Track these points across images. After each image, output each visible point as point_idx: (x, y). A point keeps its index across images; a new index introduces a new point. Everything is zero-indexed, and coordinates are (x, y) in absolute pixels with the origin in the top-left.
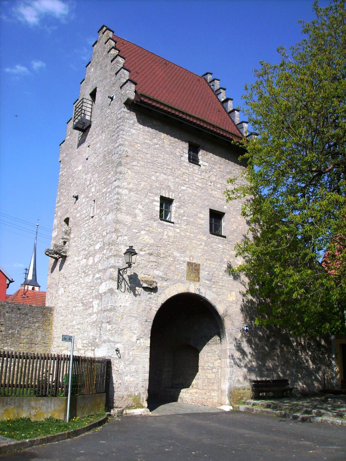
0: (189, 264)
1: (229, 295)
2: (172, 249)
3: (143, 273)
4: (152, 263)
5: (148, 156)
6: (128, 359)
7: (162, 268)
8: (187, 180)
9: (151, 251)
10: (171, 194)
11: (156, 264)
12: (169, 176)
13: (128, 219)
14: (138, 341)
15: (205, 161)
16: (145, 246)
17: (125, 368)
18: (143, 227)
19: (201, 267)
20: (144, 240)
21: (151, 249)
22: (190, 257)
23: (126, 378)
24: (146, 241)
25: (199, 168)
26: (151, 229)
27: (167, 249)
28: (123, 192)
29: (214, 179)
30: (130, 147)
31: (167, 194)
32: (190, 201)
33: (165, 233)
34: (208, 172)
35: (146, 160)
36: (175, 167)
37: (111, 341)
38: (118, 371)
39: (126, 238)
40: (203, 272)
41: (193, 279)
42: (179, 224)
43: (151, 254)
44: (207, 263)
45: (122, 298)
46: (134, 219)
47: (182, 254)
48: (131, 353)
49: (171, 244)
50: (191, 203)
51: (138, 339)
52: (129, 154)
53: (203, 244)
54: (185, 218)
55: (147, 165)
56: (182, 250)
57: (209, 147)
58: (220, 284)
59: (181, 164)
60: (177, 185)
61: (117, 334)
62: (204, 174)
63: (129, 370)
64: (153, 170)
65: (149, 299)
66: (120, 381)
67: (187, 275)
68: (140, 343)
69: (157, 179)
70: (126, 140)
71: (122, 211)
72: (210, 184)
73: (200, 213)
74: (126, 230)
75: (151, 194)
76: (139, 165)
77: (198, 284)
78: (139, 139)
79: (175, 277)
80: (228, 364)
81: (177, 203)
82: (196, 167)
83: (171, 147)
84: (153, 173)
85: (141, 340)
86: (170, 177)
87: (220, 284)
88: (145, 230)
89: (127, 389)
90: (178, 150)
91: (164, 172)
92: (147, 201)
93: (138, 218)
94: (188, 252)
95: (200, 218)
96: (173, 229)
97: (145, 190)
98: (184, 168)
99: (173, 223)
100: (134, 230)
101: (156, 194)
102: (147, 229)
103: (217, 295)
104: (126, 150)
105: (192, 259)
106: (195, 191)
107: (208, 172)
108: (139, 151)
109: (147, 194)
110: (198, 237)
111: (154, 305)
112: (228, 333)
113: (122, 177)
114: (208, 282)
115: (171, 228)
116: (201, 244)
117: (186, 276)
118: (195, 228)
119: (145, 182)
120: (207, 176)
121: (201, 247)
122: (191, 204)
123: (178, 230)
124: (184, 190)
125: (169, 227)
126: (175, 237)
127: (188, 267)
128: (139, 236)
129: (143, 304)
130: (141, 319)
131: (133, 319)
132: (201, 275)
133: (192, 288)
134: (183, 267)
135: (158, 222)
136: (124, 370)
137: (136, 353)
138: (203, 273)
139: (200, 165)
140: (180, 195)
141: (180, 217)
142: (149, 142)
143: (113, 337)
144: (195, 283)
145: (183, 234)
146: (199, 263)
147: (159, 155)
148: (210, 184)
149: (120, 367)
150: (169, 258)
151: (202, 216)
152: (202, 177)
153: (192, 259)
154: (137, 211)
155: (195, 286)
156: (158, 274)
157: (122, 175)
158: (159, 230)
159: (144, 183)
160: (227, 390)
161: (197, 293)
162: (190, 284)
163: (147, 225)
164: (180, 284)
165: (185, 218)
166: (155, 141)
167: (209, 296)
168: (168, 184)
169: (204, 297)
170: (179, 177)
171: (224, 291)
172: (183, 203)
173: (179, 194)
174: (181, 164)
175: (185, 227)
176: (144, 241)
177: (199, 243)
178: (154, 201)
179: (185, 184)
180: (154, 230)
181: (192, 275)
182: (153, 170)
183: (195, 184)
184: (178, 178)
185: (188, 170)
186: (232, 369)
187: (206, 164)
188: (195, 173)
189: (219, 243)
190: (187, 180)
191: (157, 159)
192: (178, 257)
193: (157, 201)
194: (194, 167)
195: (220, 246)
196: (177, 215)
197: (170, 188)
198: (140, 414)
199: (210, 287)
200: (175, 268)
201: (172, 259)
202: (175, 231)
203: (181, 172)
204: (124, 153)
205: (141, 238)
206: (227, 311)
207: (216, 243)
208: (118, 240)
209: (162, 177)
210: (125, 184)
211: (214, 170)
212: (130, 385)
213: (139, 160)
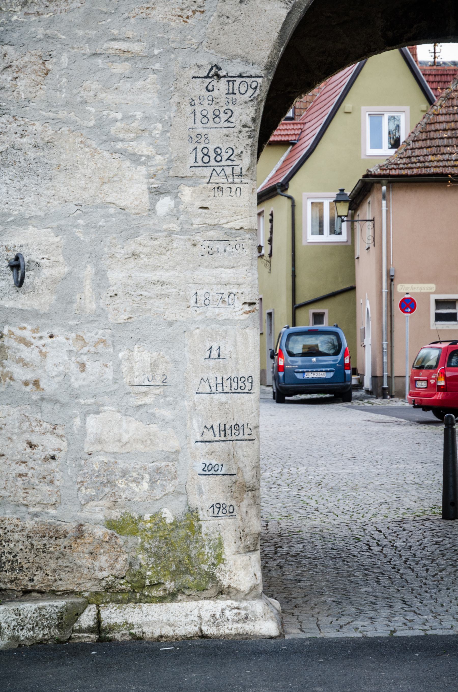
6: (100, 314)
14: (165, 204)
17: (83, 367)
23: (92, 422)
38: (36, 383)
48: (116, 276)
51: (157, 192)
63: (109, 374)
66: (51, 443)
68: (174, 214)
85: (187, 193)
89: (106, 481)
136: (78, 381)
149: (49, 362)
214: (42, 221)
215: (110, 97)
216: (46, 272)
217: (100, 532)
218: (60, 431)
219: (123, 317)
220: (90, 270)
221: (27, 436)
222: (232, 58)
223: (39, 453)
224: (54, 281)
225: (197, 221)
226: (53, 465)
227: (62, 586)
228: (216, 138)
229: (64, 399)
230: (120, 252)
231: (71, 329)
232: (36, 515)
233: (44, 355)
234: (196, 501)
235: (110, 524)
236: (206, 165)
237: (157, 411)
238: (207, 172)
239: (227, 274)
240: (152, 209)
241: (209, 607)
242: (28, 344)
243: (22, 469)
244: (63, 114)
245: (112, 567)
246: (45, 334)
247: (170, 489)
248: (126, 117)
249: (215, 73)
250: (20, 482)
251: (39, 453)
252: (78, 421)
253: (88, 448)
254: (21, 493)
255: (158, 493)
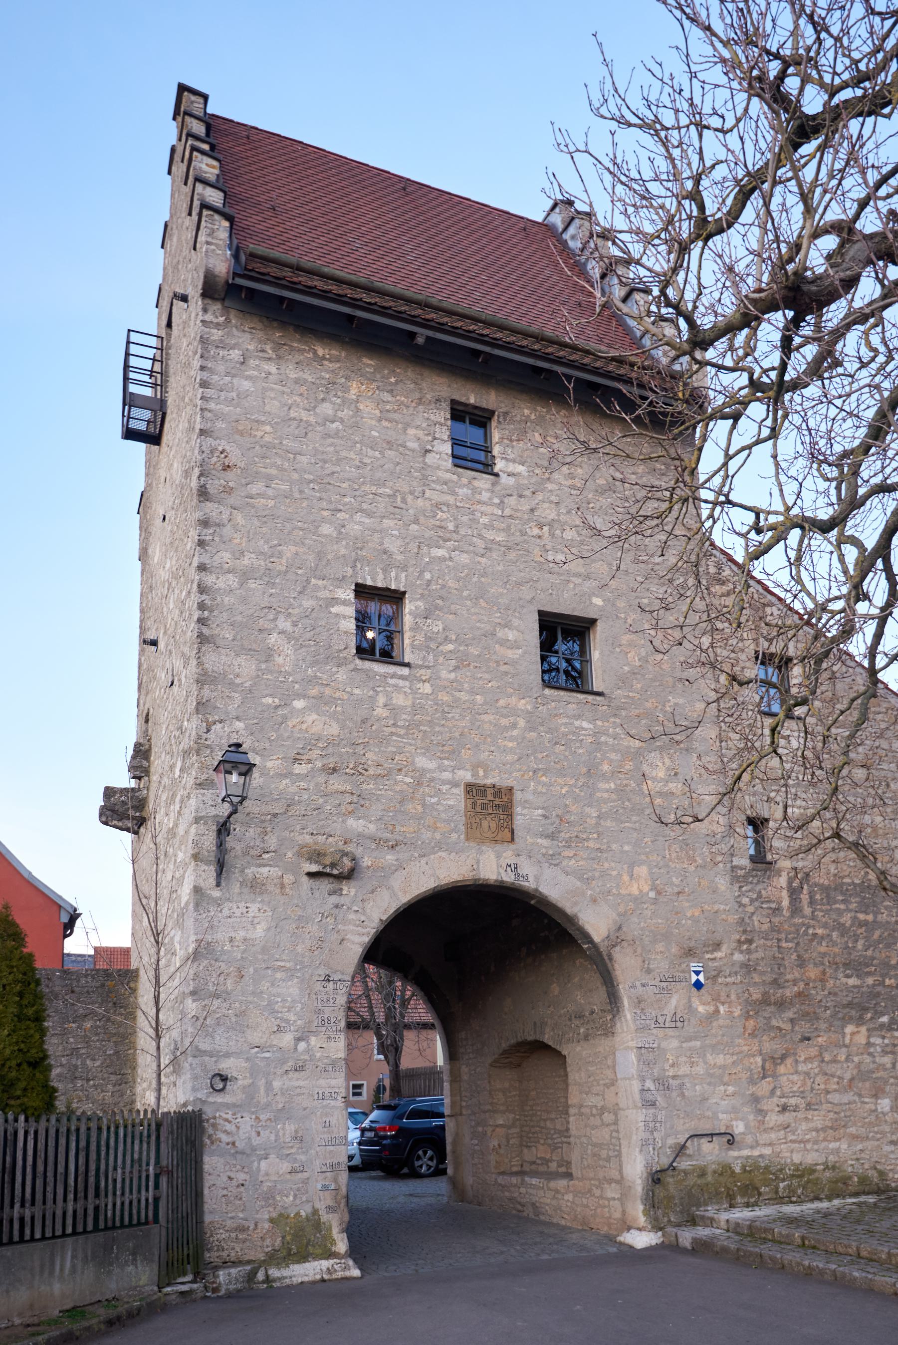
0: (472, 789)
1: (626, 878)
2: (408, 748)
3: (309, 830)
4: (340, 796)
5: (304, 459)
6: (268, 1105)
7: (376, 810)
8: (451, 526)
9: (331, 762)
10: (393, 574)
11: (355, 799)
12: (383, 517)
13: (245, 668)
14: (302, 1046)
15: (514, 461)
16: (310, 745)
17: (258, 1134)
18: (297, 686)
19: (518, 796)
20: (304, 726)
21: (332, 754)
22: (475, 768)
23: (264, 1164)
24: (314, 730)
25: (493, 485)
26: (328, 691)
27: (390, 749)
28: (221, 584)
29: (548, 513)
30: (237, 437)
31: (381, 576)
32: (465, 594)
33: (381, 700)
34: (527, 493)
35: (295, 476)
36: (406, 489)
37: (204, 1053)
38: (233, 1144)
39: (239, 725)
40: (525, 812)
41: (489, 835)
42: (428, 667)
43: (334, 770)
44: (539, 782)
45: (238, 913)
46: (263, 666)
47: (446, 762)
48: (277, 1084)
49: (402, 732)
50: (468, 597)
51: (298, 1040)
52: (232, 459)
53: (522, 723)
54: (451, 647)
55: (301, 492)
56: (446, 749)
57: (526, 412)
58: (591, 844)
59: (425, 477)
60: (413, 547)
61: (222, 1028)
62: (512, 501)
63: (273, 1138)
64: (324, 504)
65: (336, 911)
66: (241, 1177)
67: (469, 826)
68: (308, 1051)
69: (340, 533)
70: (218, 416)
71: (220, 642)
72: (536, 531)
73: (507, 625)
74: (237, 702)
75: (320, 583)
76: (270, 492)
77: (508, 855)
78: (267, 408)
79: (426, 835)
80: (637, 1096)
81: (420, 603)
82: (483, 481)
83: (385, 423)
84: (325, 513)
85: (313, 1040)
86: (387, 522)
87: (591, 844)
88: (304, 697)
89: (269, 1197)
90: (411, 431)
91: (365, 506)
92: (308, 603)
93: (280, 660)
94: (465, 754)
95: (504, 642)
96: (407, 683)
97: (300, 572)
98: (438, 487)
99: (407, 665)
100: (269, 700)
101: (341, 581)
102: (314, 692)
103: (580, 879)
104: (220, 449)
105: (481, 773)
106: (483, 560)
107: (527, 493)
108: (268, 446)
109: (308, 582)
110: (502, 703)
111: (351, 927)
112: (630, 997)
113: (212, 534)
114: (544, 842)
115: (401, 683)
116: (514, 726)
117: (463, 828)
118: (487, 676)
119: (295, 544)
120: (526, 507)
121: (515, 733)
122: (468, 603)
123: (427, 688)
124: (442, 559)
125: (392, 681)
126: (416, 709)
127: (470, 802)
128: (285, 718)
129: (313, 928)
130: (307, 976)
131: (279, 975)
132: (519, 821)
133: (490, 866)
134: (451, 802)
135: (352, 666)
136: (256, 1141)
137: (297, 1084)
138: (522, 817)
139: (497, 475)
140: (428, 576)
141: (433, 645)
142: (304, 415)
143: (208, 1040)
144: (499, 847)
145: (444, 697)
146: (510, 783)
147: (344, 454)
148: (536, 531)
149: (241, 1132)
150: (399, 778)
151: (511, 635)
152: (507, 512)
153: (481, 773)
154: (273, 639)
155: (498, 857)
156: (360, 830)
157: (211, 531)
158: (357, 691)
159: (293, 549)
160: (639, 1181)
161: (508, 878)
162: (481, 852)
163: (312, 681)
164: (443, 854)
165: (451, 647)
166: (326, 409)
167: (552, 884)
168: (381, 544)
169: (536, 890)
170: (422, 519)
171: (606, 865)
172: (440, 602)
173: (422, 572)
174: (425, 477)
175: (452, 676)
176: (306, 731)
177: (504, 722)
178: (335, 601)
179: (445, 541)
180: (338, 695)
181: (485, 824)
182: (324, 504)
183: (480, 536)
184: (416, 521)
185: (454, 493)
186: (652, 1111)
187: (520, 469)
188: (479, 502)
189: (579, 717)
190: (451, 526)
191: (338, 469)
192: (430, 771)
193: (345, 603)
194: (476, 483)
195: (585, 724)
196: (420, 638)
197: (390, 556)
198: (318, 1277)
199: (553, 859)
200: (424, 806)
201: (408, 780)
202: (414, 692)
203: (428, 504)
204: (214, 459)
205: (295, 721)
206: (620, 928)
207: (568, 717)
208: (212, 735)
209: (357, 525)
210: (226, 556)
211: (550, 486)
212: (279, 1187)
213: (270, 478)
214: (237, 1054)
215: (274, 990)
216: (240, 1082)
217: (267, 1225)
218: (246, 1170)
219: (280, 1106)
220: (263, 1080)
221: (229, 1173)
222: (335, 972)
223: (234, 1183)
224: (244, 1087)
225: (318, 1055)
226: (242, 1189)
227: (246, 1258)
228: (328, 1012)
229: (248, 1151)
230: (279, 1072)
231: (253, 1113)
232: (232, 1218)
233: (238, 1128)
234: (318, 1205)
235: (271, 1220)
236: (323, 1025)
237: (298, 1157)
238: (324, 1029)
239: (333, 1082)
240: (296, 1049)
241: (325, 1264)
242: (230, 1122)
243: (225, 1192)
244: (250, 998)
245: (273, 1245)
246: (239, 1116)
247: (304, 1199)
248: (284, 1000)
249: (327, 979)
250: (223, 1200)
251: (234, 1183)
252: (256, 1164)
253: (260, 1179)
254: (224, 1206)
255: (298, 1202)
